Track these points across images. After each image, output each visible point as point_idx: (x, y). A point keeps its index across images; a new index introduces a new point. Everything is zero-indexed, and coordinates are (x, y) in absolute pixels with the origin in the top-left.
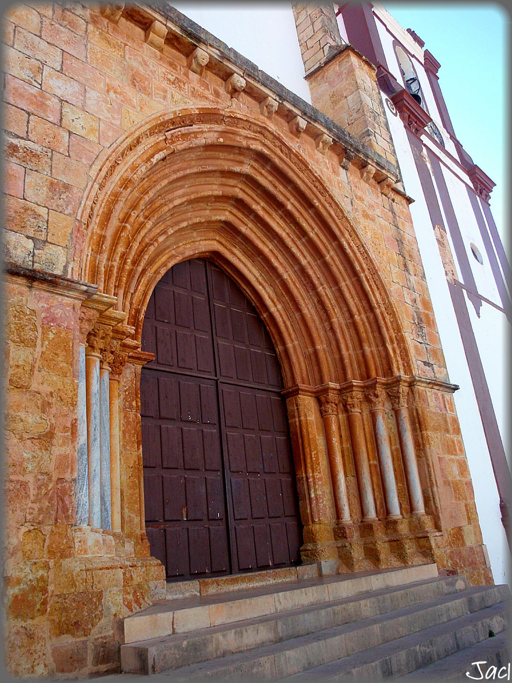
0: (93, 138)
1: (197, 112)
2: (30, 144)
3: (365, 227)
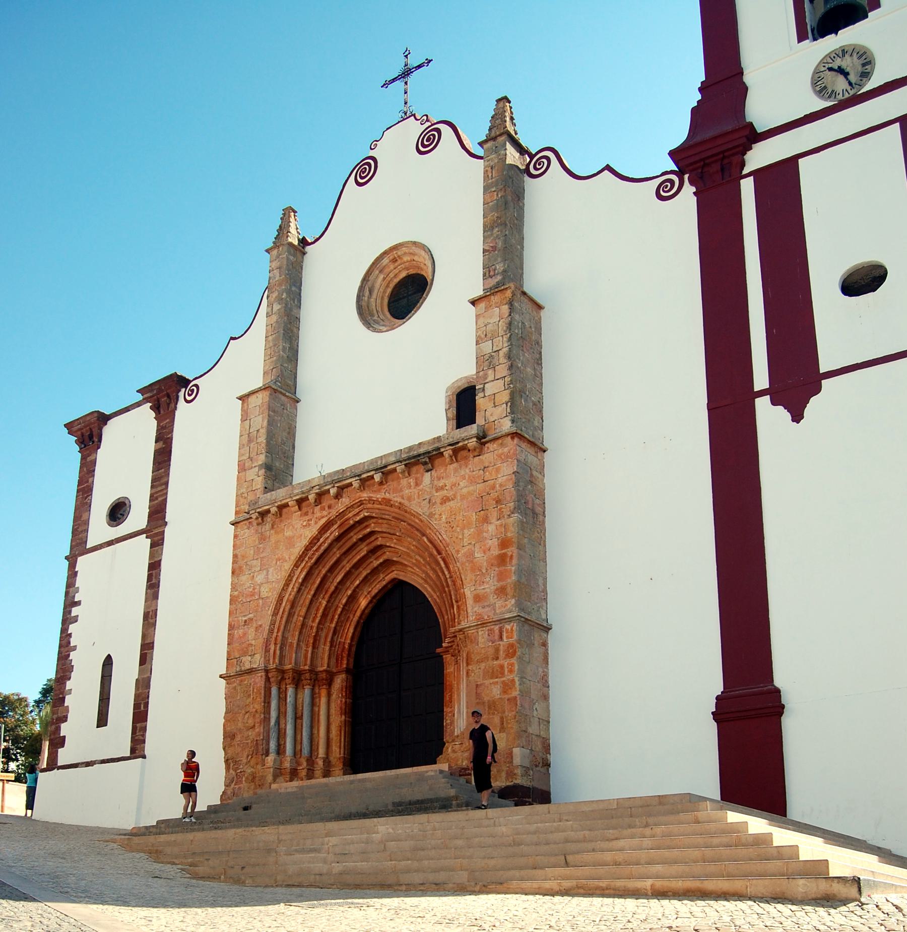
1: (317, 533)
2: (251, 615)
3: (440, 515)
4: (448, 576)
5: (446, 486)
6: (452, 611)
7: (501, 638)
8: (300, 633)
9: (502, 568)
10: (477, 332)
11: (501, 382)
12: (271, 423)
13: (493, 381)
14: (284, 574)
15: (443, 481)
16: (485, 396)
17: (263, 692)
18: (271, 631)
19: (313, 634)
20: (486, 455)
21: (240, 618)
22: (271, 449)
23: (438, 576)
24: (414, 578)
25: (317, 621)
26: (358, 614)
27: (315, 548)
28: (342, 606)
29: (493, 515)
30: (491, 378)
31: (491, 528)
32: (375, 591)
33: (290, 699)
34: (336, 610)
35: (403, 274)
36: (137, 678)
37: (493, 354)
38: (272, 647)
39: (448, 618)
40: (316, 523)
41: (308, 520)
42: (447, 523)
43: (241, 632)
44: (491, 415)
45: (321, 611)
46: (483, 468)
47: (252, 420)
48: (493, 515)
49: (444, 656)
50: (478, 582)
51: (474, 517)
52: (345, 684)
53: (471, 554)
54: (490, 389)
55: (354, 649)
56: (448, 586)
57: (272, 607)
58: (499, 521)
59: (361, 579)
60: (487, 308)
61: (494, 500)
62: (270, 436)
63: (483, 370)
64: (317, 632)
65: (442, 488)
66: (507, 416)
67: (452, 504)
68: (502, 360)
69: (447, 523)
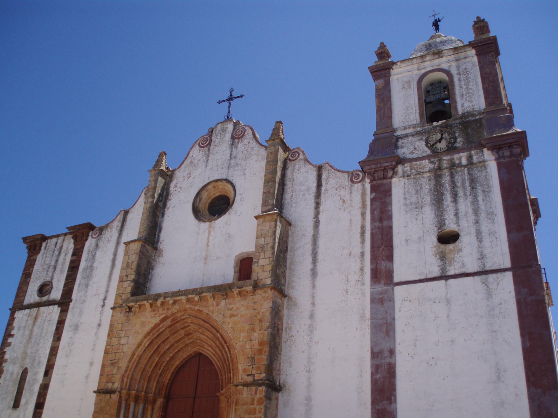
0: (128, 351)
3: (228, 323)
4: (229, 356)
5: (233, 308)
6: (229, 375)
7: (256, 393)
8: (142, 374)
9: (260, 357)
10: (257, 233)
11: (267, 260)
12: (140, 258)
13: (263, 259)
14: (138, 341)
15: (232, 306)
16: (258, 266)
17: (117, 404)
18: (126, 371)
19: (149, 375)
20: (257, 296)
21: (109, 361)
22: (138, 272)
23: (223, 354)
24: (209, 352)
25: (152, 368)
26: (174, 367)
27: (157, 330)
28: (166, 362)
29: (257, 327)
30: (262, 257)
31: (256, 335)
32: (185, 356)
33: (131, 410)
34: (162, 363)
35: (218, 194)
36: (41, 383)
37: (264, 245)
38: (125, 380)
39: (226, 377)
40: (159, 316)
41: (155, 314)
42: (232, 328)
43: (109, 369)
44: (261, 276)
45: (155, 363)
46: (254, 302)
47: (130, 256)
48: (257, 327)
49: (220, 397)
50: (246, 362)
51: (247, 327)
52: (162, 405)
53: (243, 347)
54: (261, 262)
55: (169, 385)
56: (228, 360)
57: (128, 358)
58: (260, 332)
59: (179, 349)
60: (263, 222)
61: (258, 320)
62: (139, 266)
63: (258, 252)
64: (151, 374)
65: (231, 309)
66: (269, 278)
67: (235, 318)
68: (269, 249)
69: (232, 328)
